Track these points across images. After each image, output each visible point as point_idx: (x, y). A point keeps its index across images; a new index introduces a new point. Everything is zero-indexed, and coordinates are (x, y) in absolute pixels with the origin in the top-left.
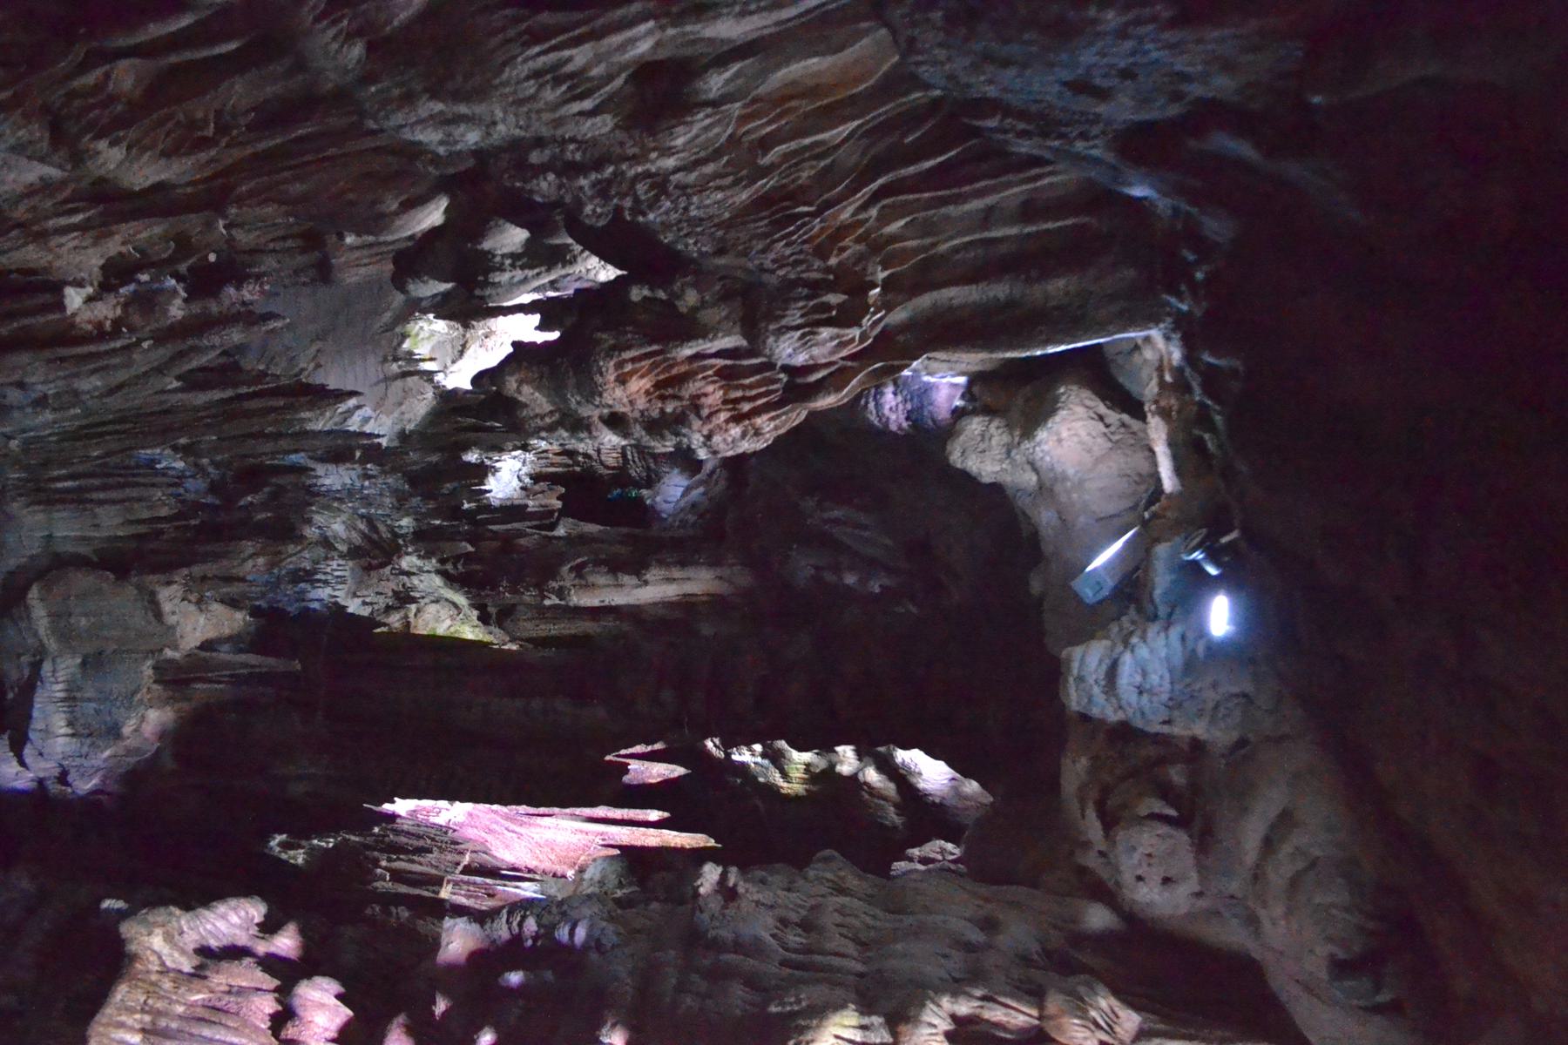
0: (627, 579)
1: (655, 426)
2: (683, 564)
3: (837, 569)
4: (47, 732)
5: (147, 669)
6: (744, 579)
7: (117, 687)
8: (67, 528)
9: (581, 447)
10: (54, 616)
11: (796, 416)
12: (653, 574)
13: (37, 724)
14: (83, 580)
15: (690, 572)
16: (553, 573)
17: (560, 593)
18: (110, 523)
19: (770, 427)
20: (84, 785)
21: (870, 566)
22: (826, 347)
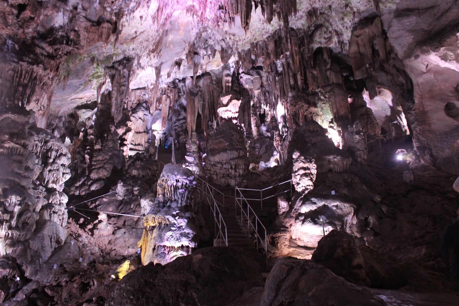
0: (255, 125)
1: (275, 139)
2: (257, 131)
3: (258, 148)
4: (246, 76)
5: (252, 87)
6: (255, 138)
7: (251, 84)
8: (264, 79)
9: (269, 116)
10: (257, 78)
11: (276, 147)
12: (256, 128)
13: (246, 75)
14: (260, 81)
15: (256, 132)
16: (255, 116)
17: (253, 116)
18: (265, 83)
19: (275, 146)
20: (241, 80)
21: (259, 152)
22: (280, 149)
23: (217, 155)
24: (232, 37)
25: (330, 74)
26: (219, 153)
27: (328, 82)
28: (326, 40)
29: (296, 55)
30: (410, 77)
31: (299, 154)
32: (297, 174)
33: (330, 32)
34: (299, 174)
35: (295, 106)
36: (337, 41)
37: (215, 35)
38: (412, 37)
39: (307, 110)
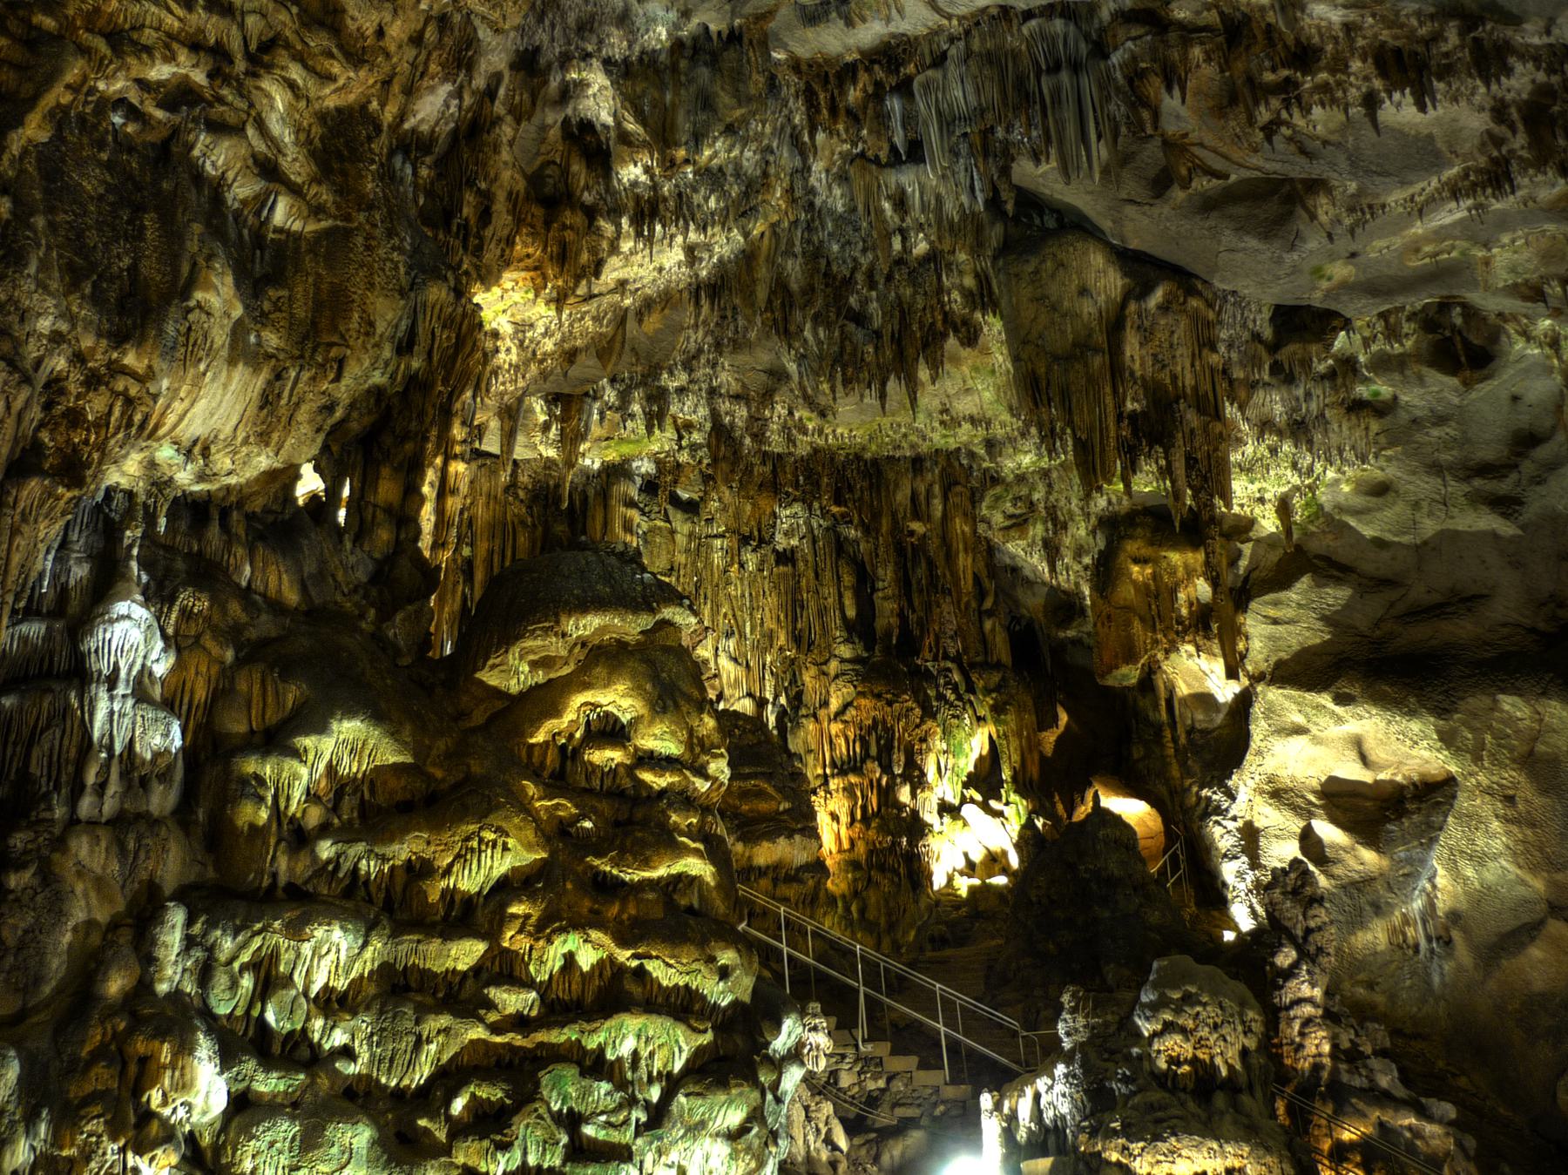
23: (766, 844)
24: (797, 415)
25: (993, 630)
26: (771, 836)
27: (986, 653)
28: (1007, 523)
29: (966, 550)
30: (1252, 727)
31: (1294, 954)
32: (1292, 1013)
33: (1032, 505)
34: (1295, 1017)
35: (890, 704)
36: (1038, 539)
37: (719, 368)
38: (1328, 637)
39: (918, 726)
